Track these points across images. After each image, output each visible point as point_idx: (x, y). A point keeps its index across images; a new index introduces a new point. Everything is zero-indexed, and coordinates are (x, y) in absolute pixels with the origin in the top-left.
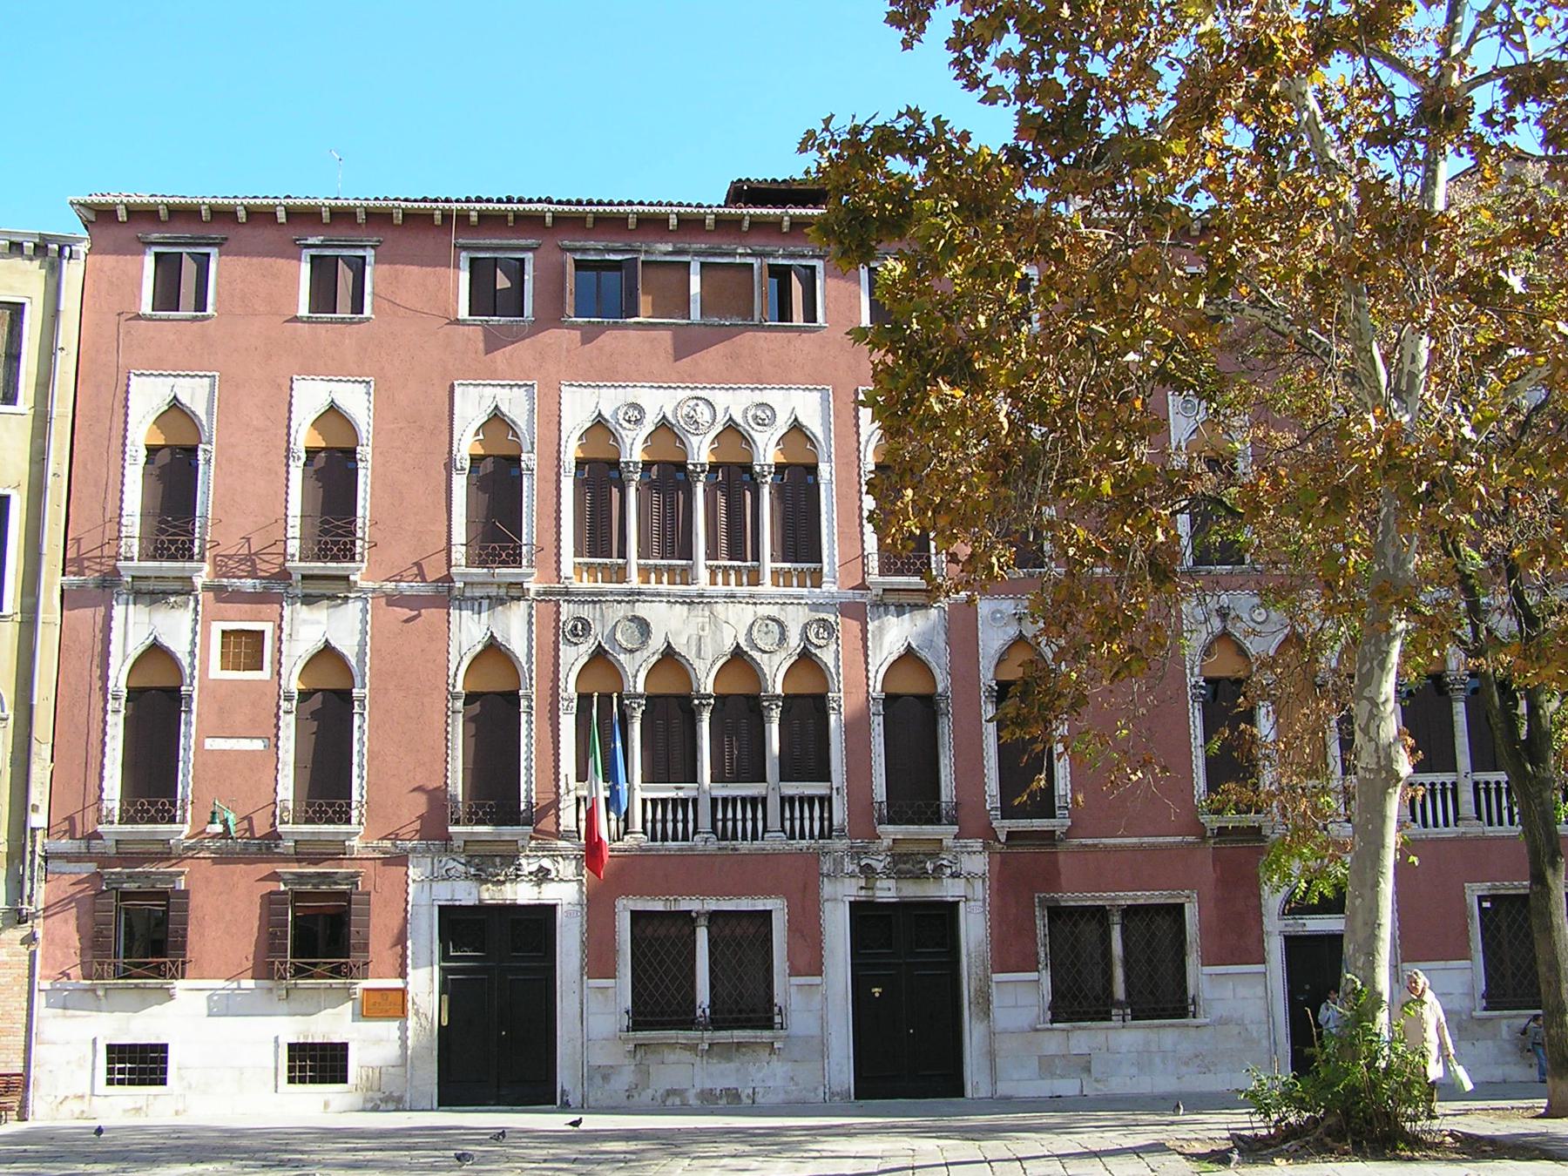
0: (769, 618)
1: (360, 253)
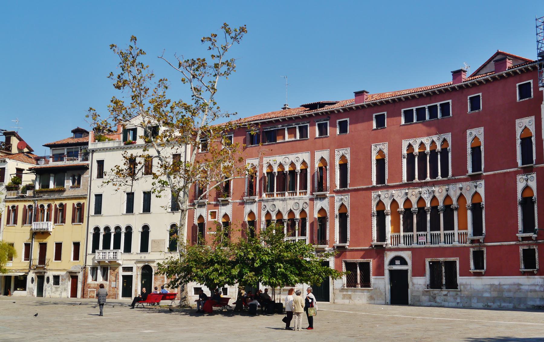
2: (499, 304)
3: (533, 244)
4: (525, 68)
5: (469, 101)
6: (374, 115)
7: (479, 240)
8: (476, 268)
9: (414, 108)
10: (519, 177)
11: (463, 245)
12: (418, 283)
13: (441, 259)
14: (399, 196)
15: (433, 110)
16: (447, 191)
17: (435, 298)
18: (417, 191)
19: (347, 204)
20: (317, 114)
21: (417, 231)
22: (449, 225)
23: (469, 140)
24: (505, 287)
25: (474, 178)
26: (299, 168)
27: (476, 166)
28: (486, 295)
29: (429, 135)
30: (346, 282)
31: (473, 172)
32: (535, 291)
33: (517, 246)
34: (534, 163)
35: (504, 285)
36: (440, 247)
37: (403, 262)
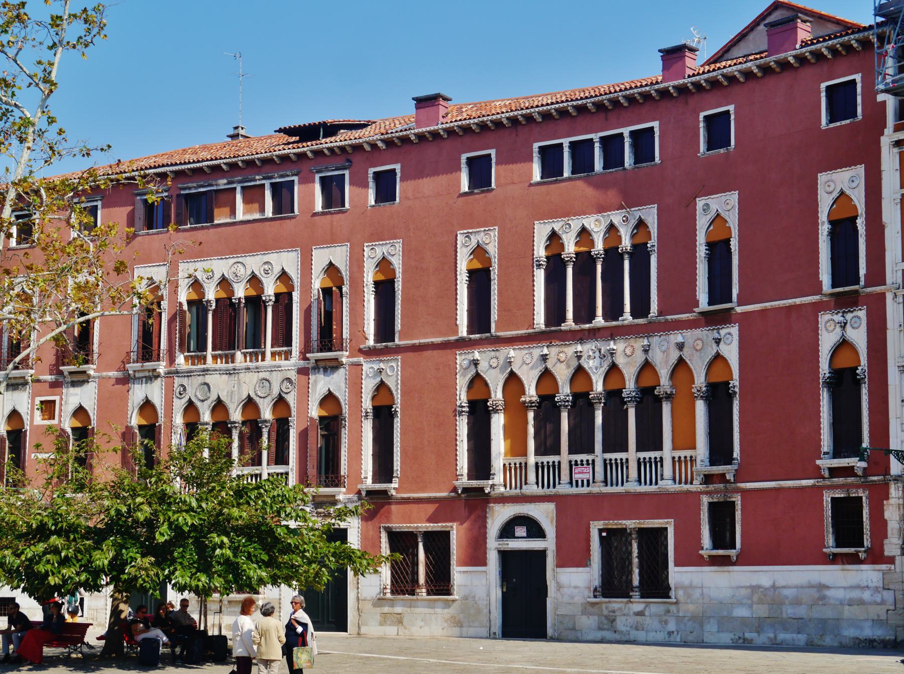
0: (264, 379)
1: (95, 203)
2: (772, 635)
3: (858, 487)
4: (842, 45)
5: (702, 125)
6: (464, 157)
7: (723, 475)
8: (715, 546)
9: (566, 142)
10: (824, 318)
11: (685, 487)
12: (570, 586)
13: (631, 524)
14: (526, 363)
15: (612, 146)
16: (646, 351)
17: (613, 621)
18: (571, 350)
19: (394, 383)
20: (318, 153)
21: (571, 452)
22: (650, 438)
23: (702, 223)
24: (786, 592)
25: (714, 320)
26: (270, 289)
27: (719, 289)
28: (741, 612)
29: (601, 209)
30: (389, 582)
31: (710, 304)
32: (861, 602)
33: (817, 491)
34: (862, 283)
35: (784, 587)
36: (627, 494)
37: (535, 530)
